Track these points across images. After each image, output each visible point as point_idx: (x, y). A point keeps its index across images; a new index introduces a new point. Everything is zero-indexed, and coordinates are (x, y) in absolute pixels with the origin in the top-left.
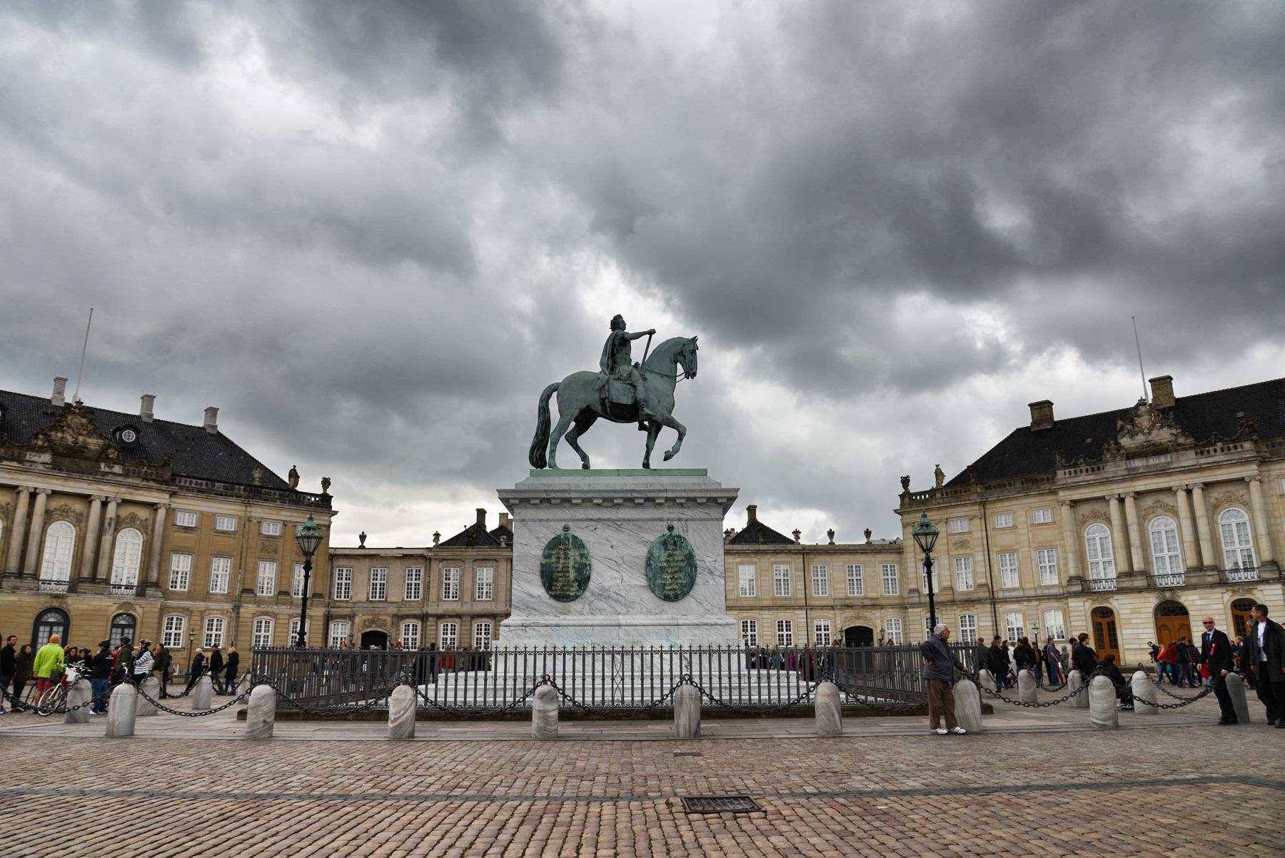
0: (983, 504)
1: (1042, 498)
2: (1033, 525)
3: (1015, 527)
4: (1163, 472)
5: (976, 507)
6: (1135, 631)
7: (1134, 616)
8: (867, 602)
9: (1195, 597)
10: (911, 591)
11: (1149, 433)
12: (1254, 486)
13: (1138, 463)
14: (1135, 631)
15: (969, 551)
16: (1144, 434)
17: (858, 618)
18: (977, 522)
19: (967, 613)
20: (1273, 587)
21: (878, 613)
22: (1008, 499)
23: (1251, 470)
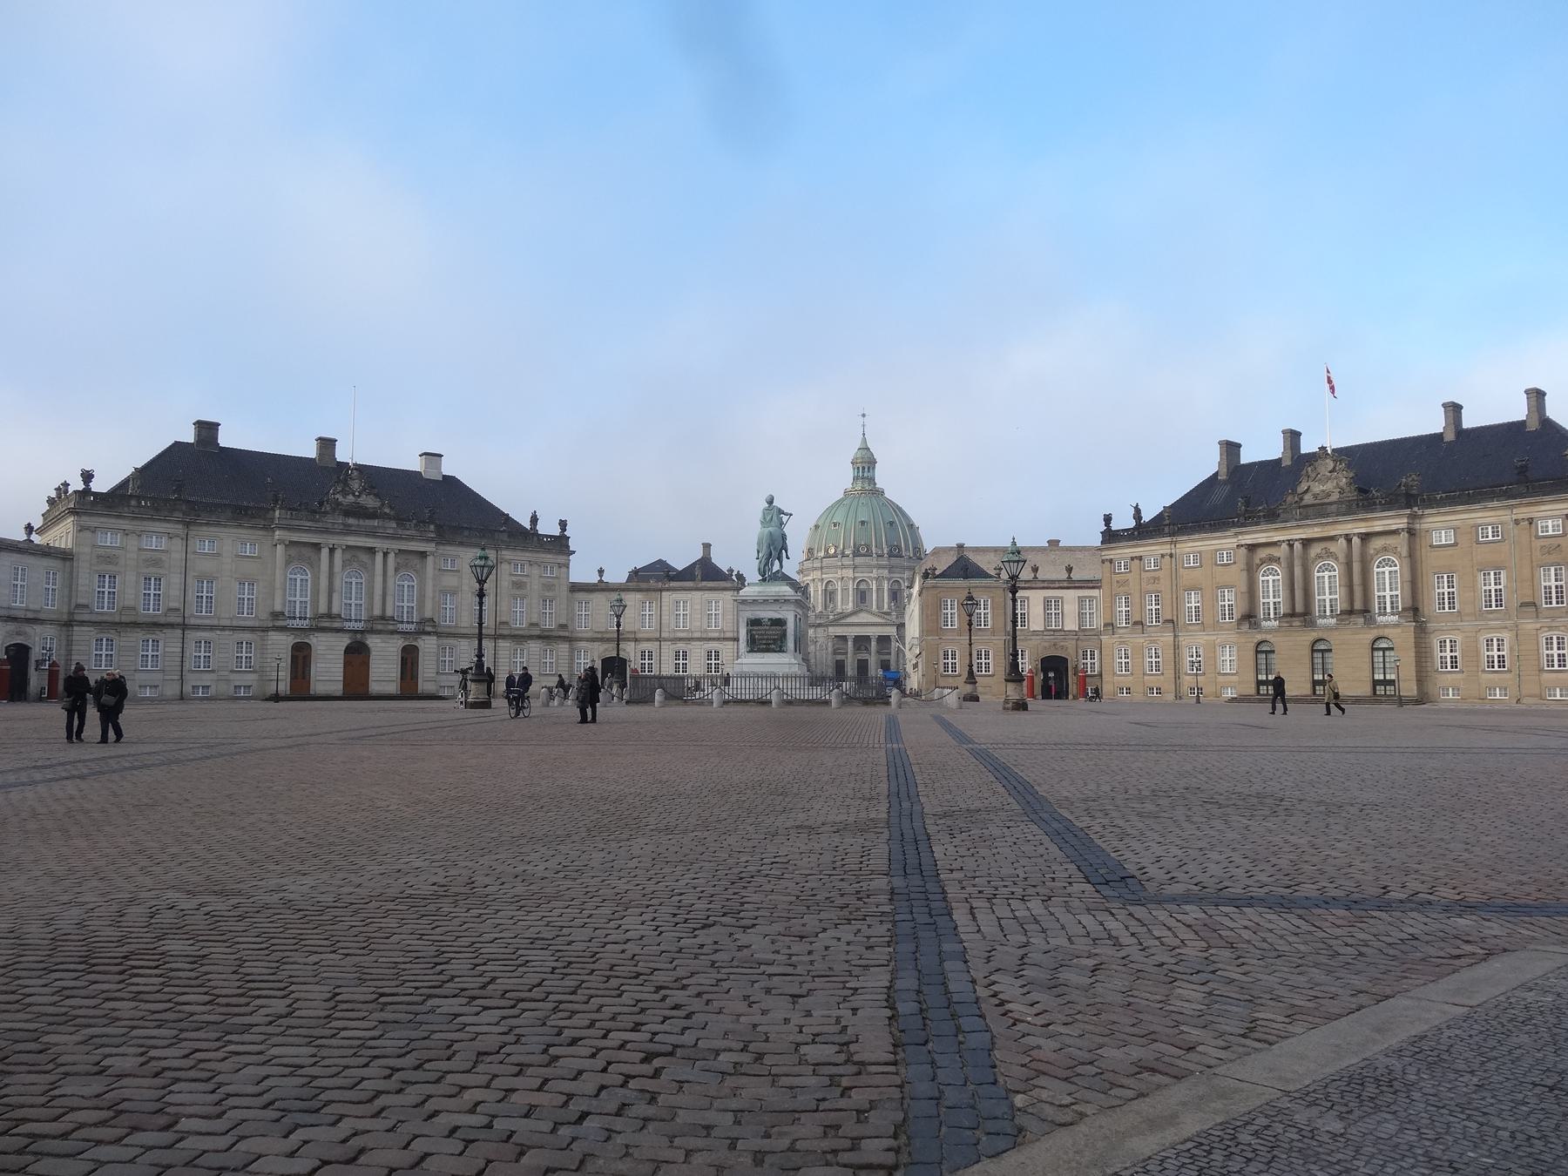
0: (187, 525)
1: (250, 531)
2: (237, 556)
3: (218, 555)
4: (372, 533)
5: (181, 526)
6: (328, 665)
7: (328, 652)
8: (30, 615)
9: (379, 641)
10: (78, 606)
11: (359, 496)
12: (430, 559)
13: (351, 521)
14: (328, 665)
15: (161, 571)
16: (354, 495)
17: (18, 634)
18: (178, 544)
19: (151, 637)
20: (431, 638)
21: (38, 628)
22: (218, 524)
23: (429, 547)
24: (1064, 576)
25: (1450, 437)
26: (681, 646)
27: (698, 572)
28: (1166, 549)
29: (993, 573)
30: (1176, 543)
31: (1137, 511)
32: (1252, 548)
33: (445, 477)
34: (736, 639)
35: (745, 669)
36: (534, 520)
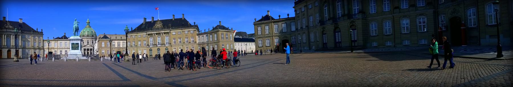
24: (120, 38)
25: (173, 19)
26: (61, 50)
27: (63, 37)
28: (136, 34)
29: (110, 38)
30: (137, 33)
31: (132, 28)
32: (149, 34)
33: (23, 23)
34: (69, 49)
35: (71, 53)
36: (37, 29)
